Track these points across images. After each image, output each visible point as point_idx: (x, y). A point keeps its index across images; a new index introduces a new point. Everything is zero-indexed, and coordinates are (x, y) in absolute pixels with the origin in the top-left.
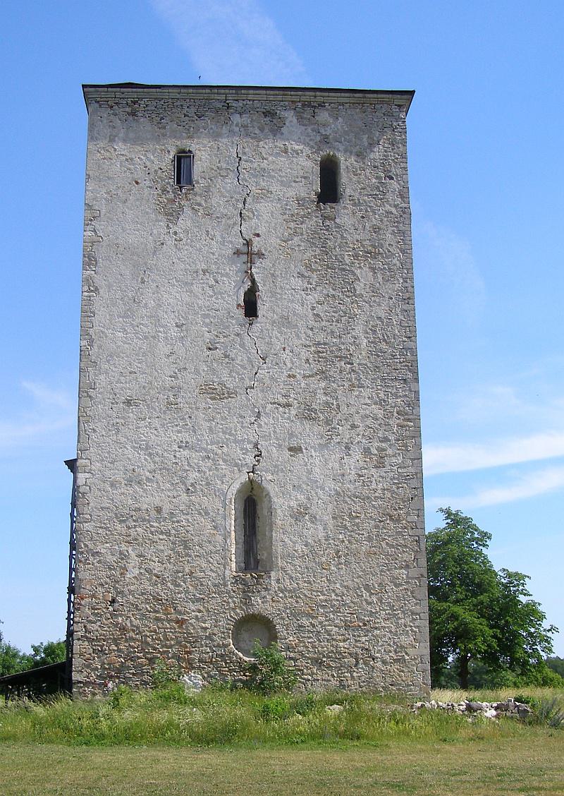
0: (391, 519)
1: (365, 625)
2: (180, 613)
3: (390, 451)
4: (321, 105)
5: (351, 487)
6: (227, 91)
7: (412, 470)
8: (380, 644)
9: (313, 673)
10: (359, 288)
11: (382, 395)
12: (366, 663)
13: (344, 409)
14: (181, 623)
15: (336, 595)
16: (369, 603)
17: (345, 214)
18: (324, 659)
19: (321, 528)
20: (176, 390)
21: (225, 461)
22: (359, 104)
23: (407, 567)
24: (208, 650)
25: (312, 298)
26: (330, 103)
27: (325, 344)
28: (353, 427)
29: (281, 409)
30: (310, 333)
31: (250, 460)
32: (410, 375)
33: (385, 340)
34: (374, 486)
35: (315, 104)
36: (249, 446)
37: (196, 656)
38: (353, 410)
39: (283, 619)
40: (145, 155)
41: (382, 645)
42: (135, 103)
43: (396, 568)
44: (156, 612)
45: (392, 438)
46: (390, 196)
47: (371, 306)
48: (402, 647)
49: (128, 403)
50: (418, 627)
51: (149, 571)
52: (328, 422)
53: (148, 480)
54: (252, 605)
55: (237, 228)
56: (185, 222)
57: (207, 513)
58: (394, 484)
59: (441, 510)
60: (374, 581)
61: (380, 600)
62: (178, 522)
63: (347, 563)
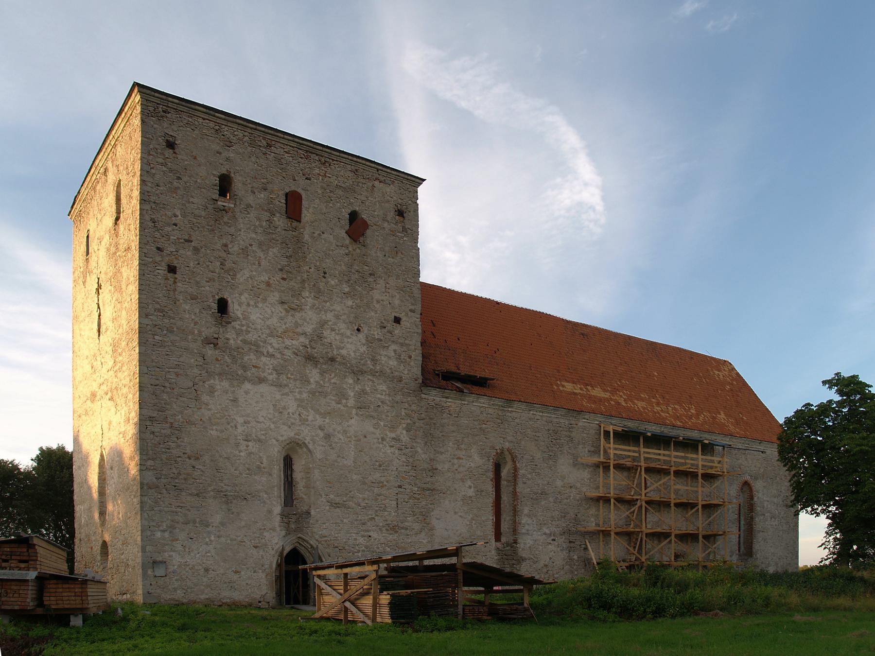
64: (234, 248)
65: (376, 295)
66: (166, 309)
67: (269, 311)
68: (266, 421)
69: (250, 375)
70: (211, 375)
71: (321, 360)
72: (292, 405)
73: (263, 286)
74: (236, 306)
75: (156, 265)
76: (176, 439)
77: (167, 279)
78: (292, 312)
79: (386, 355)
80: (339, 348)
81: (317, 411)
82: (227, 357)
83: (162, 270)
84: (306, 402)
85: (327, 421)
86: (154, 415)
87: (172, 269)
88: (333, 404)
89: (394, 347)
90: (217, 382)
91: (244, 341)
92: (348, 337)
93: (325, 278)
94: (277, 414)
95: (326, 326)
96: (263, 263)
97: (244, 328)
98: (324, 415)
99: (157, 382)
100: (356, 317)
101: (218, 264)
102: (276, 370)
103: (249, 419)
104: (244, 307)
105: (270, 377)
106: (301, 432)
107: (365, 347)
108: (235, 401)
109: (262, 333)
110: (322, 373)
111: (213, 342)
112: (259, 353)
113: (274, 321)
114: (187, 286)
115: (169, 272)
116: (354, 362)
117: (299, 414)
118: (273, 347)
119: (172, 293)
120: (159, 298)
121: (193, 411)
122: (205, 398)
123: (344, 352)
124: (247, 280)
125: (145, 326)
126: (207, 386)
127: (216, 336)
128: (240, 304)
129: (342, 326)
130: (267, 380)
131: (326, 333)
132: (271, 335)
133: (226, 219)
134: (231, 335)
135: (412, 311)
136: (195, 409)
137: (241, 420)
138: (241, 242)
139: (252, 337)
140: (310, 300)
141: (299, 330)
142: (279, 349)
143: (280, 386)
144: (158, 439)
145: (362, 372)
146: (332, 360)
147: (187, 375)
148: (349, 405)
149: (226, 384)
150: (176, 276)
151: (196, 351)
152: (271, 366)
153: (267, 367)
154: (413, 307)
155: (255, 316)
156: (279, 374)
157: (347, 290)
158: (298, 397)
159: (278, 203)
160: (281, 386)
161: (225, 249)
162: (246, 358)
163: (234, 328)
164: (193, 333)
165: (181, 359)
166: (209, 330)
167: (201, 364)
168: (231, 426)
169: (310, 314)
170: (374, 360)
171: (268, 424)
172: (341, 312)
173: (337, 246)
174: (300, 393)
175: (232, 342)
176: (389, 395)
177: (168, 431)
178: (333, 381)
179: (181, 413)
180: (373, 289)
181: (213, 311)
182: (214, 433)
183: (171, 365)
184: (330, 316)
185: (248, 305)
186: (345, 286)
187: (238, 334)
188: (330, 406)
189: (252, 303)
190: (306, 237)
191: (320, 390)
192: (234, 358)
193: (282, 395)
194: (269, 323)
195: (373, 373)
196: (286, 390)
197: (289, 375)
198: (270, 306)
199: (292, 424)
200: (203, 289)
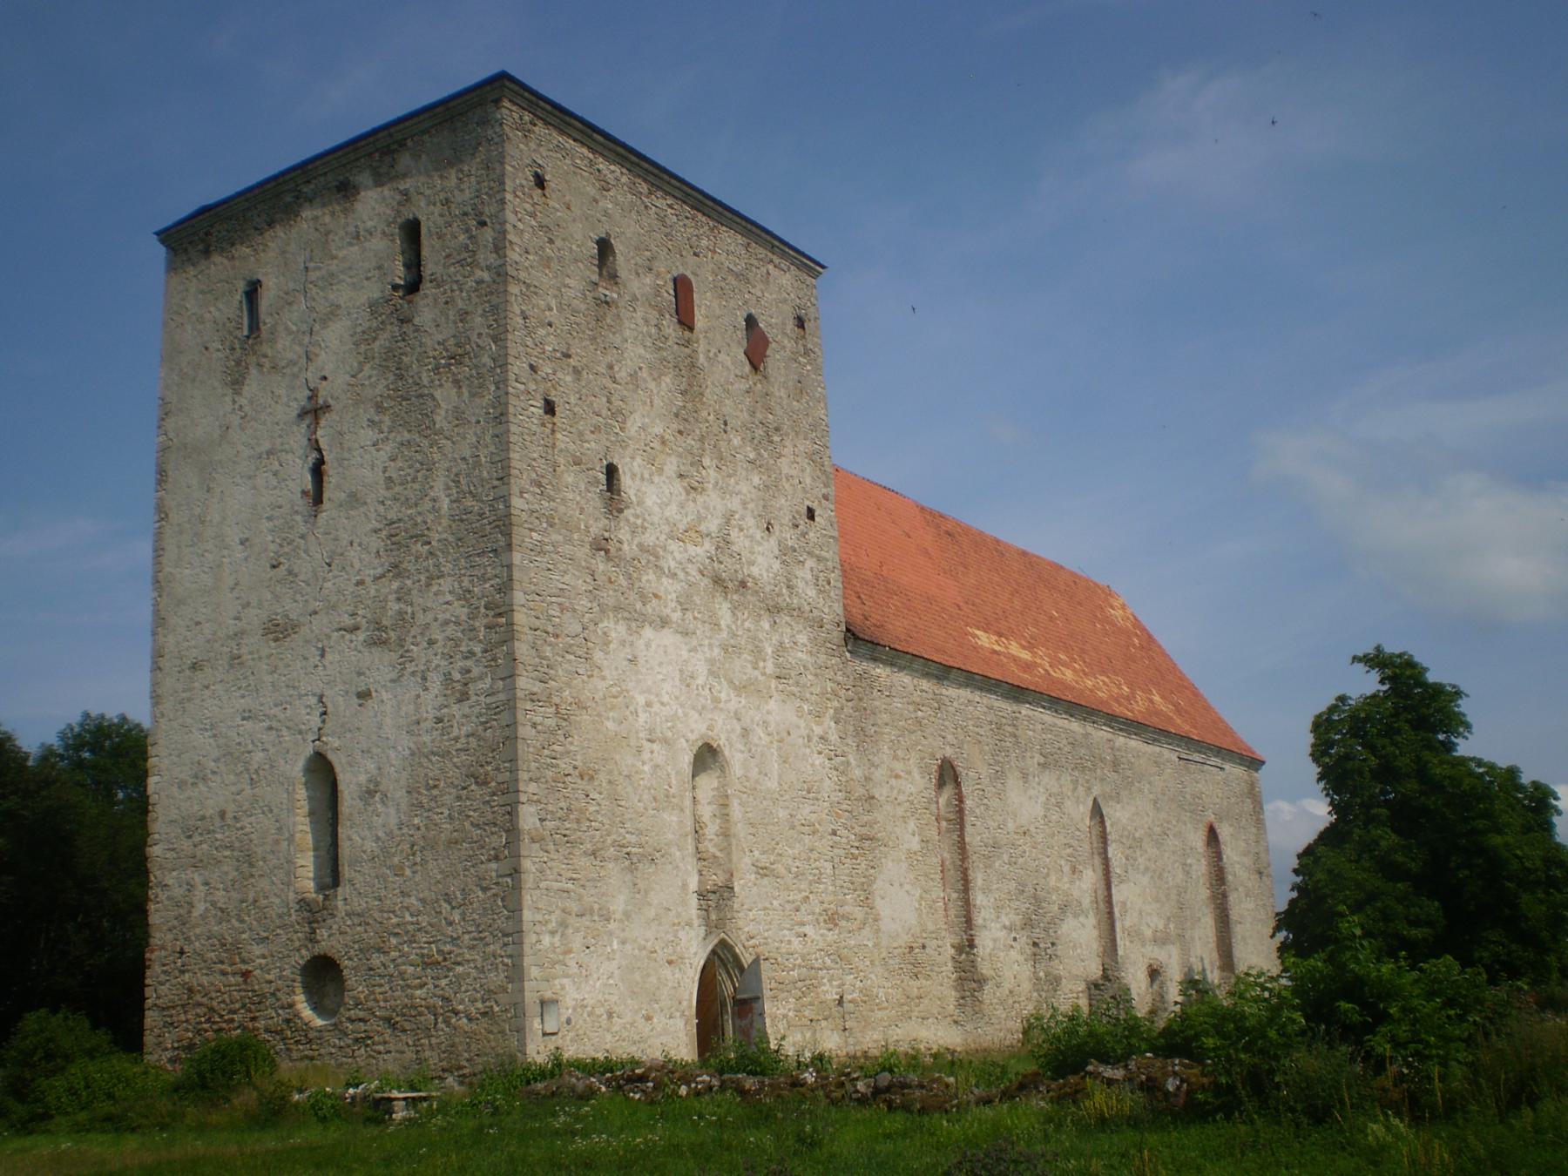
0: (477, 783)
1: (445, 959)
2: (243, 961)
3: (476, 672)
4: (402, 144)
5: (426, 738)
6: (293, 175)
7: (502, 697)
8: (463, 989)
9: (385, 1043)
10: (440, 419)
11: (466, 584)
12: (447, 1022)
13: (421, 619)
14: (246, 975)
15: (412, 915)
16: (450, 924)
17: (426, 310)
18: (398, 1019)
19: (392, 811)
20: (239, 635)
21: (288, 728)
22: (447, 121)
23: (497, 858)
24: (274, 1014)
25: (388, 448)
26: (412, 137)
27: (400, 520)
28: (431, 642)
29: (348, 636)
30: (381, 509)
31: (316, 721)
32: (502, 542)
33: (471, 492)
34: (455, 733)
35: (395, 146)
36: (313, 700)
37: (261, 1024)
38: (430, 616)
39: (350, 959)
40: (214, 305)
41: (467, 991)
42: (207, 234)
43: (482, 863)
44: (222, 962)
45: (478, 649)
46: (481, 257)
47: (453, 443)
48: (490, 991)
49: (194, 667)
50: (510, 956)
51: (214, 904)
52: (401, 642)
53: (214, 773)
54: (318, 942)
55: (303, 376)
56: (251, 387)
57: (271, 811)
58: (482, 723)
59: (1355, 659)
60: (454, 888)
61: (463, 915)
62: (242, 828)
63: (424, 861)
64: (622, 375)
65: (785, 465)
66: (544, 481)
69: (650, 611)
71: (730, 585)
72: (702, 670)
73: (656, 445)
76: (562, 739)
77: (543, 425)
78: (693, 494)
79: (803, 578)
80: (752, 563)
81: (731, 682)
82: (621, 577)
84: (718, 664)
86: (535, 690)
87: (550, 408)
88: (749, 669)
89: (810, 563)
90: (612, 625)
91: (641, 546)
92: (760, 544)
93: (725, 432)
96: (657, 401)
98: (740, 689)
99: (537, 623)
101: (605, 399)
102: (681, 604)
103: (652, 697)
105: (676, 616)
106: (714, 723)
107: (778, 561)
108: (633, 661)
110: (734, 610)
111: (601, 546)
113: (672, 512)
114: (568, 440)
115: (546, 413)
116: (767, 589)
117: (710, 689)
118: (674, 559)
119: (550, 451)
120: (534, 460)
122: (598, 656)
123: (755, 570)
127: (606, 535)
128: (634, 475)
129: (751, 522)
132: (671, 536)
135: (826, 497)
136: (585, 678)
139: (649, 539)
140: (711, 472)
144: (541, 737)
147: (574, 611)
148: (768, 671)
149: (622, 628)
150: (555, 420)
152: (674, 595)
153: (670, 597)
154: (824, 491)
155: (651, 501)
157: (752, 456)
158: (708, 655)
159: (666, 295)
160: (687, 634)
161: (610, 372)
162: (644, 578)
163: (628, 520)
165: (566, 579)
166: (596, 528)
167: (591, 588)
168: (631, 712)
171: (674, 708)
172: (748, 495)
173: (737, 376)
175: (625, 547)
177: (551, 722)
178: (747, 624)
179: (569, 685)
180: (780, 456)
181: (601, 487)
182: (610, 725)
183: (554, 591)
184: (735, 504)
185: (642, 479)
186: (749, 449)
188: (745, 674)
190: (702, 358)
191: (732, 642)
193: (690, 651)
194: (667, 514)
197: (696, 615)
198: (667, 481)
200: (586, 445)
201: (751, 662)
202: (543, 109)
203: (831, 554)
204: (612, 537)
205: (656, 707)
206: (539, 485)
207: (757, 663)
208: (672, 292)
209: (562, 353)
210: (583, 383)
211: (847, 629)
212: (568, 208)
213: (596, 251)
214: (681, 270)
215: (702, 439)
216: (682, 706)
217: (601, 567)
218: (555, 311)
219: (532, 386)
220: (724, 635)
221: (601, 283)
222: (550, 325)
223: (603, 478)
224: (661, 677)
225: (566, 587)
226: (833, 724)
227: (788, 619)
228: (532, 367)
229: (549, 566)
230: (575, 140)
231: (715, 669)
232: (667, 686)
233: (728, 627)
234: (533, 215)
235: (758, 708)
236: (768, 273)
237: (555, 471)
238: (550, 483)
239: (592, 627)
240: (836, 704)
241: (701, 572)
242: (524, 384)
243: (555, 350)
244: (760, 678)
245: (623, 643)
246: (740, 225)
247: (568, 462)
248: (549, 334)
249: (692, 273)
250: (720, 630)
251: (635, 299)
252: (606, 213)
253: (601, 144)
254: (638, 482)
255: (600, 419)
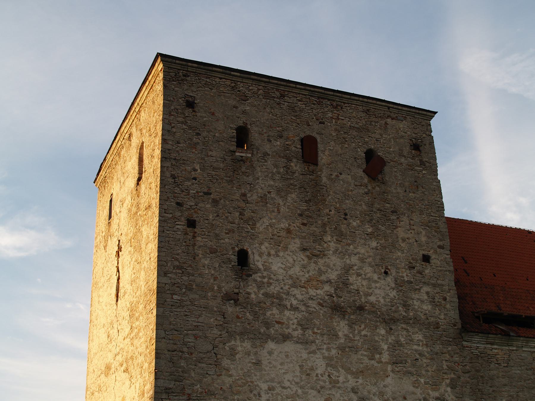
64: (253, 197)
65: (401, 233)
66: (185, 266)
67: (291, 260)
68: (292, 386)
69: (273, 332)
70: (231, 335)
71: (349, 310)
72: (321, 366)
73: (283, 234)
74: (257, 257)
75: (176, 220)
79: (418, 299)
80: (368, 295)
81: (348, 370)
82: (248, 314)
83: (181, 225)
84: (335, 359)
85: (360, 381)
87: (191, 224)
88: (366, 360)
89: (425, 289)
90: (238, 343)
91: (266, 295)
92: (376, 282)
93: (346, 219)
94: (304, 377)
95: (351, 271)
97: (266, 280)
98: (356, 374)
99: (175, 347)
100: (382, 259)
101: (237, 214)
102: (301, 325)
103: (274, 384)
104: (265, 257)
105: (295, 334)
106: (332, 396)
107: (395, 291)
108: (258, 363)
109: (285, 284)
110: (351, 325)
112: (282, 307)
113: (296, 270)
114: (206, 240)
116: (384, 309)
117: (329, 376)
118: (296, 299)
119: (191, 248)
120: (178, 254)
121: (213, 379)
122: (226, 362)
123: (372, 299)
124: (267, 228)
125: (164, 285)
126: (228, 349)
127: (236, 291)
128: (261, 255)
129: (368, 270)
130: (292, 336)
131: (352, 279)
132: (294, 285)
133: (243, 169)
134: (252, 289)
136: (215, 377)
137: (264, 386)
138: (260, 190)
139: (274, 289)
140: (332, 244)
141: (323, 278)
142: (302, 301)
143: (305, 342)
145: (394, 321)
146: (361, 308)
147: (206, 337)
148: (383, 360)
149: (247, 345)
150: (196, 230)
151: (215, 309)
152: (295, 321)
153: (291, 322)
155: (276, 265)
156: (304, 329)
157: (370, 230)
158: (326, 355)
160: (307, 343)
161: (244, 198)
162: (268, 313)
163: (255, 281)
164: (212, 290)
165: (200, 320)
166: (228, 286)
167: (221, 323)
168: (254, 395)
169: (334, 260)
170: (406, 306)
171: (295, 389)
172: (366, 254)
173: (356, 186)
174: (328, 349)
175: (253, 296)
176: (427, 345)
178: (363, 333)
179: (200, 381)
180: (397, 227)
181: (233, 264)
183: (190, 327)
184: (354, 260)
185: (269, 254)
186: (367, 226)
187: (259, 288)
188: (362, 363)
189: (273, 252)
190: (324, 180)
191: (350, 345)
192: (255, 315)
193: (310, 353)
194: (291, 272)
195: (406, 320)
196: (314, 347)
197: (316, 330)
198: (291, 254)
199: (322, 387)
200: (222, 241)
201: (367, 356)
202: (192, 67)
203: (448, 281)
204: (241, 291)
205: (278, 390)
206: (179, 267)
207: (373, 356)
208: (299, 146)
209: (204, 193)
210: (221, 207)
211: (462, 327)
212: (213, 114)
213: (235, 134)
214: (308, 133)
215: (324, 225)
216: (301, 387)
217: (230, 310)
218: (199, 171)
219: (178, 214)
220: (342, 341)
221: (238, 150)
222: (195, 179)
223: (234, 258)
224: (283, 371)
225: (200, 324)
226: (449, 389)
227: (404, 326)
228: (178, 204)
229: (186, 313)
230: (221, 78)
231: (333, 363)
232: (288, 377)
233: (345, 335)
234: (185, 123)
235: (375, 384)
236: (386, 123)
237: (194, 259)
238: (190, 266)
239: (221, 346)
240: (453, 376)
241: (320, 304)
242: (171, 213)
243: (197, 192)
244: (376, 364)
245: (248, 354)
246: (358, 100)
247: (206, 252)
248: (193, 184)
249: (317, 133)
250: (338, 338)
251: (266, 154)
252: (244, 112)
253: (240, 77)
254: (265, 257)
255: (234, 225)
